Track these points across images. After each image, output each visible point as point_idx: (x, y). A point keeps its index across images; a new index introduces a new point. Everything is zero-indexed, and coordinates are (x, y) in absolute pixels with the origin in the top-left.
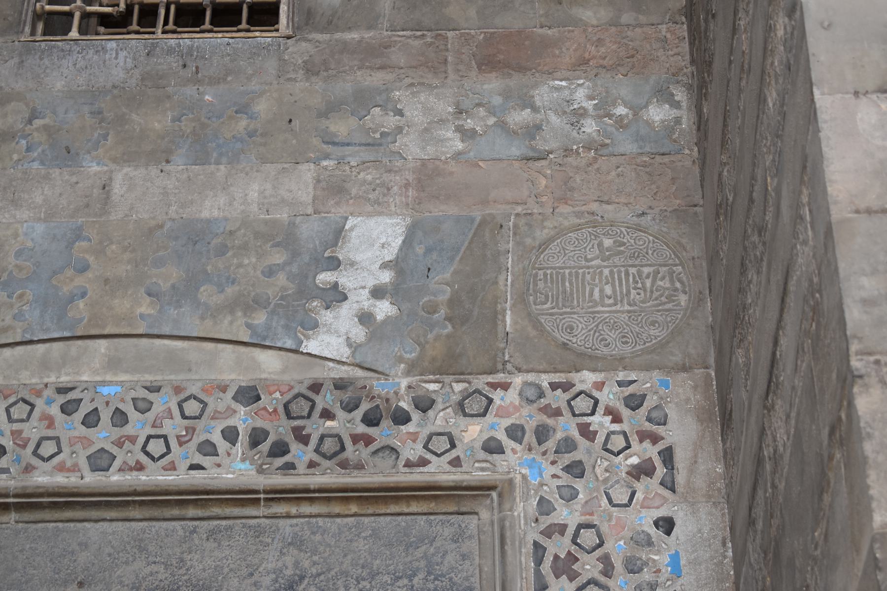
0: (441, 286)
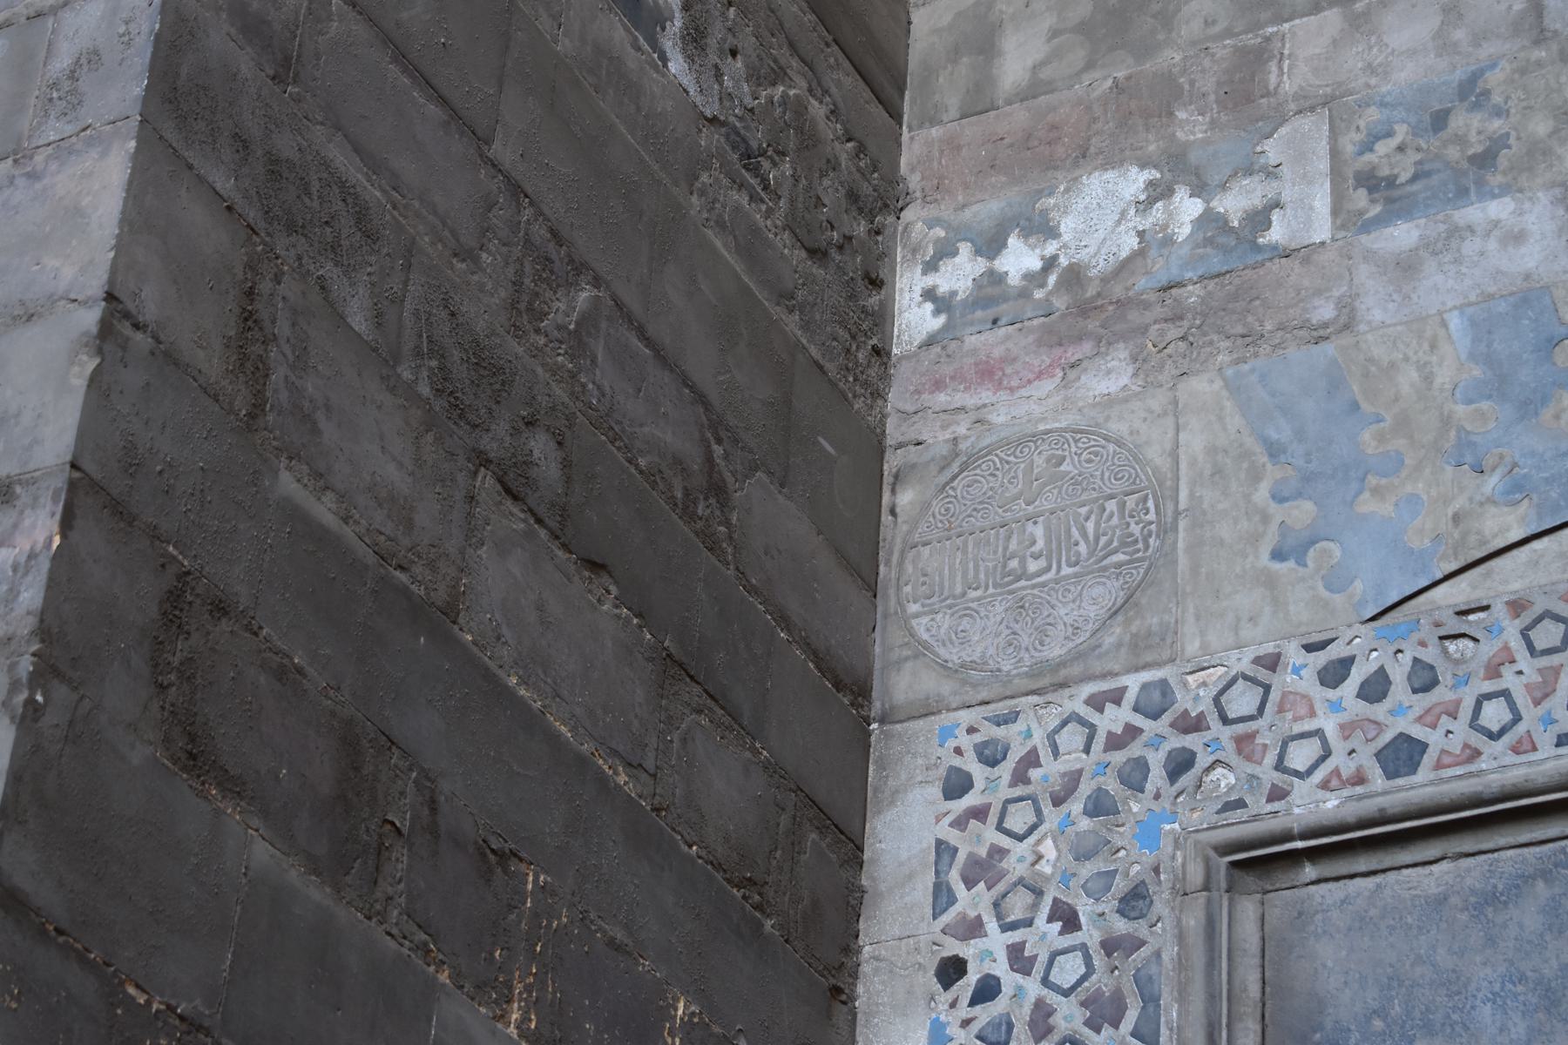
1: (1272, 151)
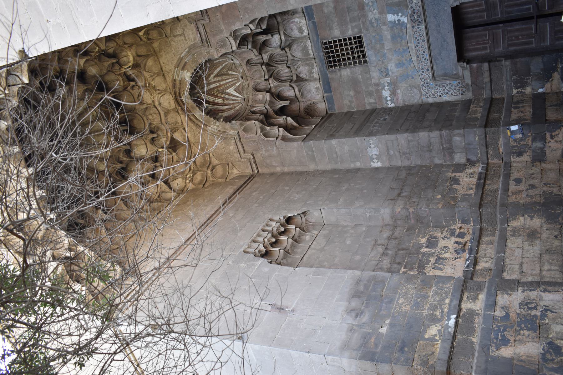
0: (396, 9)
1: (382, 82)
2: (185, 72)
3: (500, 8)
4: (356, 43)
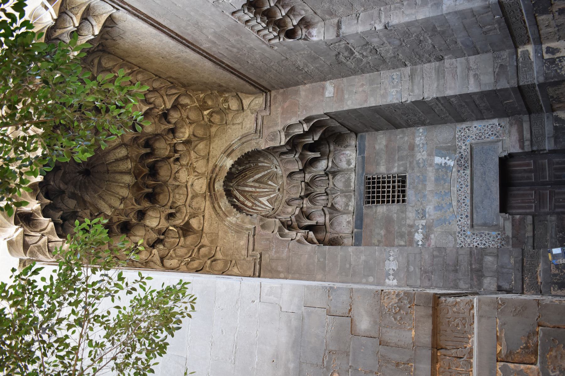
1: (417, 224)
2: (229, 159)
3: (549, 170)
4: (399, 182)
